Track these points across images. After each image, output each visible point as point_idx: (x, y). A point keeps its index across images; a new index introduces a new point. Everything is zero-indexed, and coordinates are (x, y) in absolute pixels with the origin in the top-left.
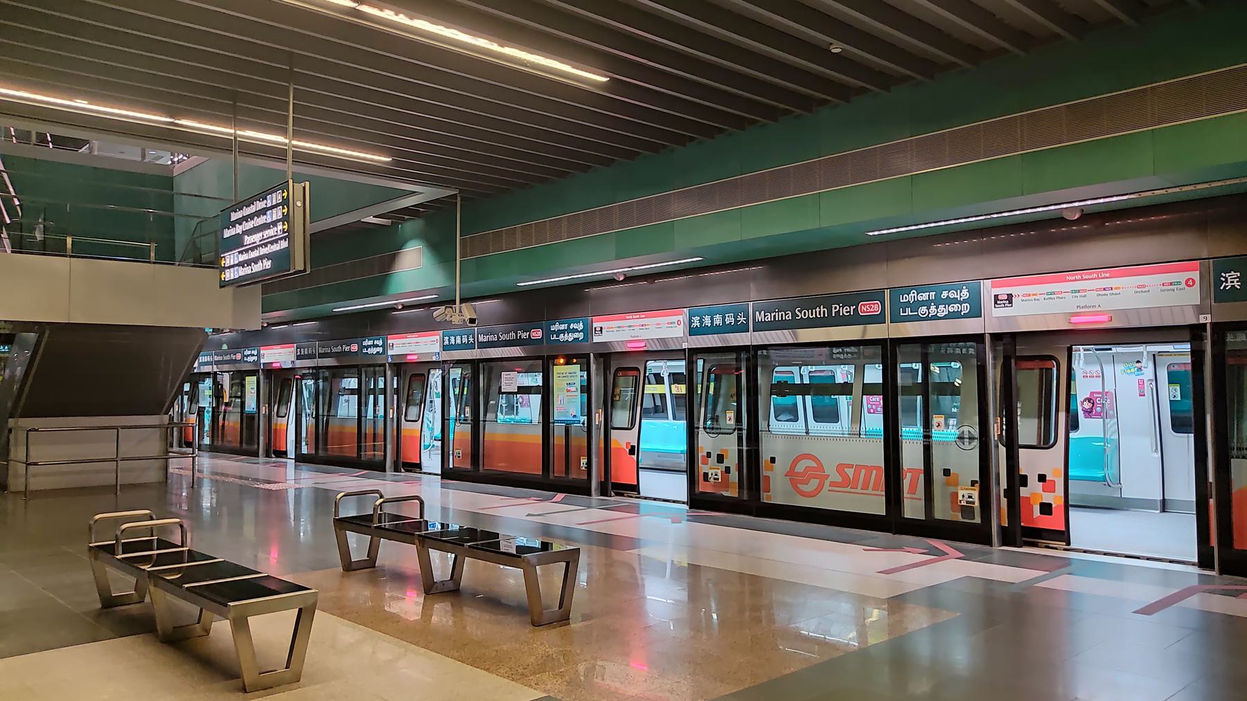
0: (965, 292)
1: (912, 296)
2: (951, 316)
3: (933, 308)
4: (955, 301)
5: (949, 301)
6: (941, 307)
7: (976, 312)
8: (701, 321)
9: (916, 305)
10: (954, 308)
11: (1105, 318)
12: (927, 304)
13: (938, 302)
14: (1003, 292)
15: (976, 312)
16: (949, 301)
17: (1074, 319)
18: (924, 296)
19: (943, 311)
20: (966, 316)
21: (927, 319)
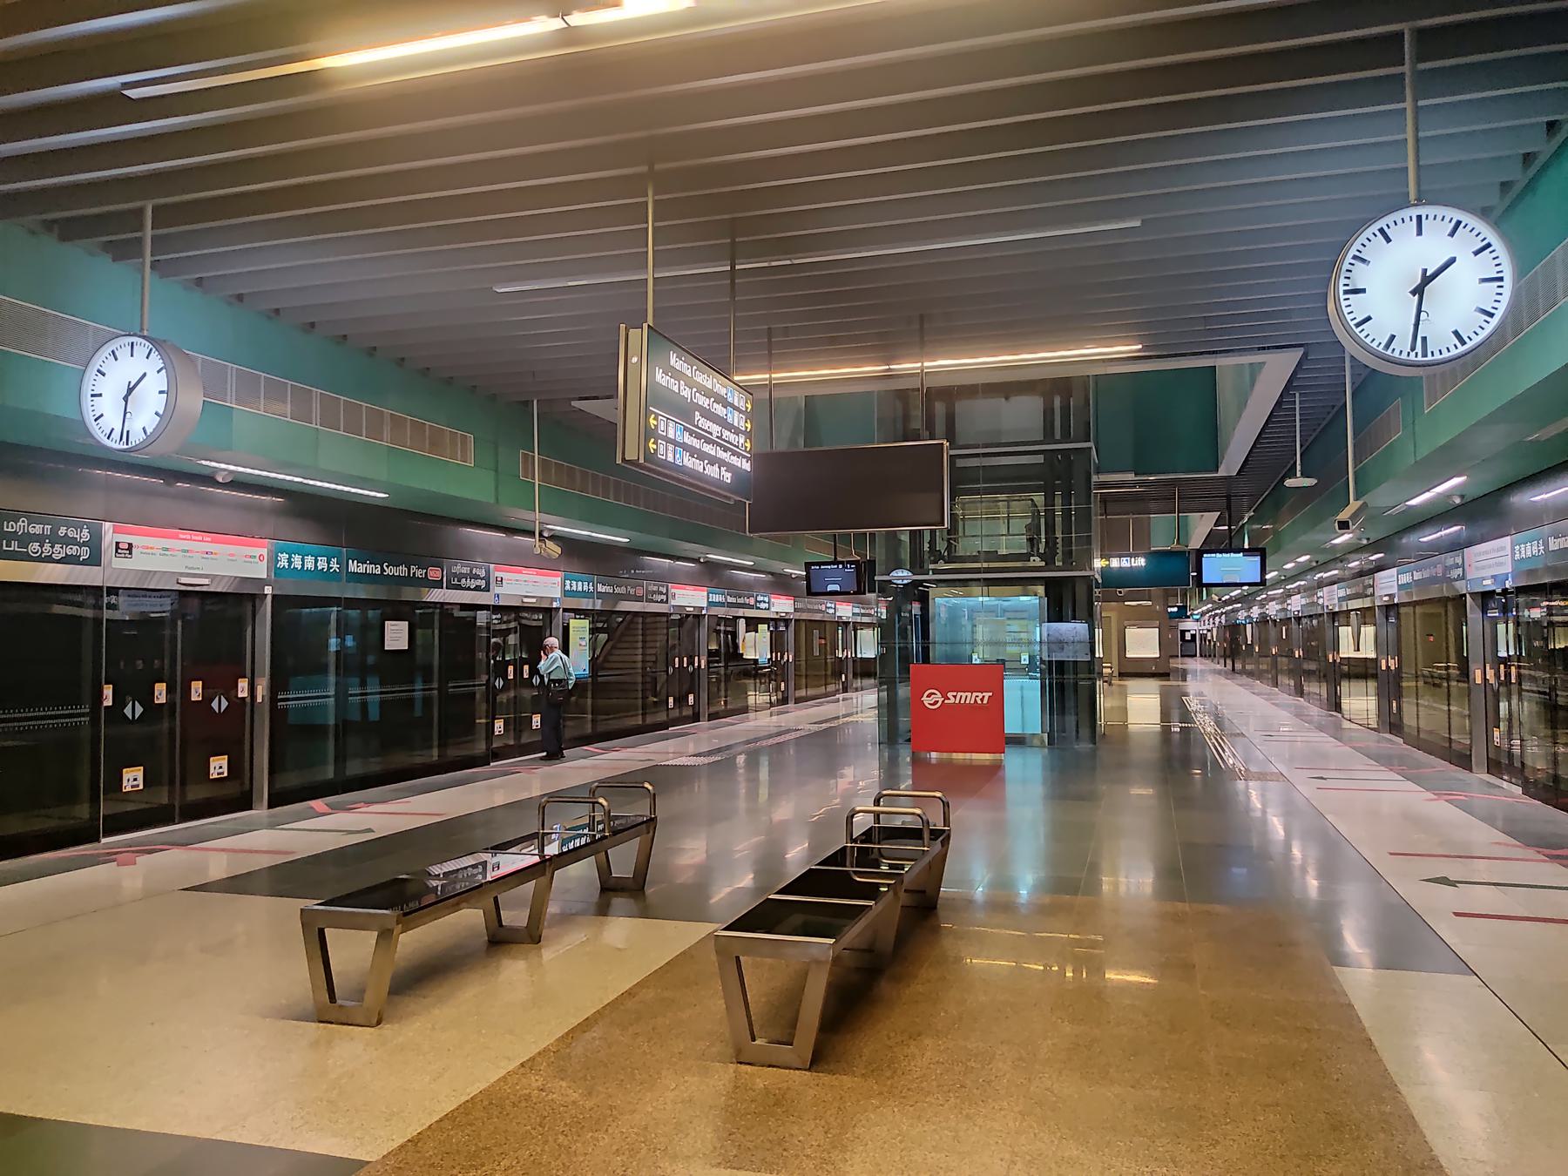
0: (85, 531)
1: (21, 526)
2: (66, 560)
3: (47, 546)
4: (74, 542)
5: (68, 541)
6: (57, 547)
7: (487, 589)
8: (290, 562)
9: (461, 576)
10: (72, 550)
11: (206, 581)
12: (465, 576)
13: (54, 539)
14: (125, 539)
15: (487, 589)
16: (68, 541)
17: (184, 580)
18: (465, 570)
19: (59, 551)
20: (84, 563)
21: (40, 559)
